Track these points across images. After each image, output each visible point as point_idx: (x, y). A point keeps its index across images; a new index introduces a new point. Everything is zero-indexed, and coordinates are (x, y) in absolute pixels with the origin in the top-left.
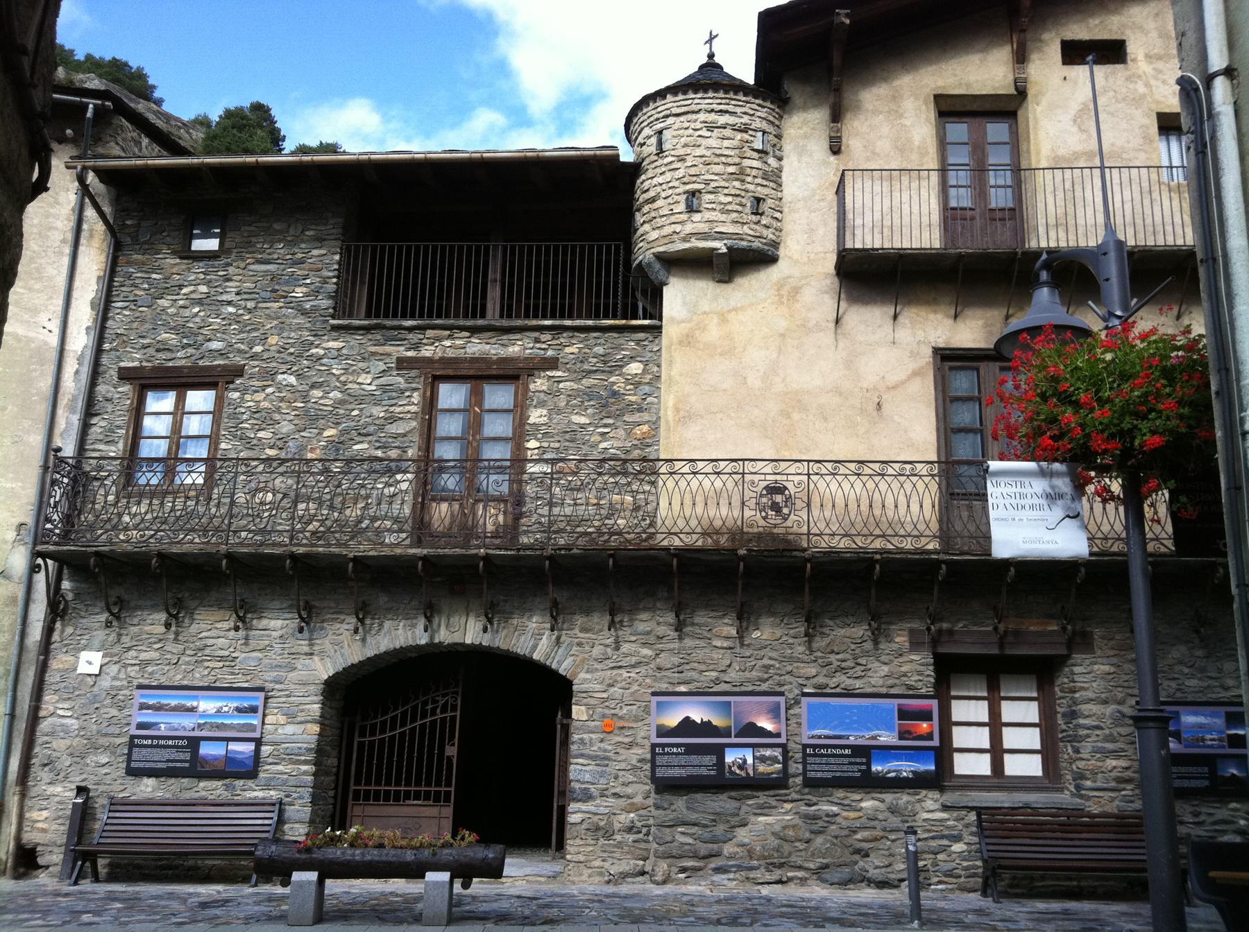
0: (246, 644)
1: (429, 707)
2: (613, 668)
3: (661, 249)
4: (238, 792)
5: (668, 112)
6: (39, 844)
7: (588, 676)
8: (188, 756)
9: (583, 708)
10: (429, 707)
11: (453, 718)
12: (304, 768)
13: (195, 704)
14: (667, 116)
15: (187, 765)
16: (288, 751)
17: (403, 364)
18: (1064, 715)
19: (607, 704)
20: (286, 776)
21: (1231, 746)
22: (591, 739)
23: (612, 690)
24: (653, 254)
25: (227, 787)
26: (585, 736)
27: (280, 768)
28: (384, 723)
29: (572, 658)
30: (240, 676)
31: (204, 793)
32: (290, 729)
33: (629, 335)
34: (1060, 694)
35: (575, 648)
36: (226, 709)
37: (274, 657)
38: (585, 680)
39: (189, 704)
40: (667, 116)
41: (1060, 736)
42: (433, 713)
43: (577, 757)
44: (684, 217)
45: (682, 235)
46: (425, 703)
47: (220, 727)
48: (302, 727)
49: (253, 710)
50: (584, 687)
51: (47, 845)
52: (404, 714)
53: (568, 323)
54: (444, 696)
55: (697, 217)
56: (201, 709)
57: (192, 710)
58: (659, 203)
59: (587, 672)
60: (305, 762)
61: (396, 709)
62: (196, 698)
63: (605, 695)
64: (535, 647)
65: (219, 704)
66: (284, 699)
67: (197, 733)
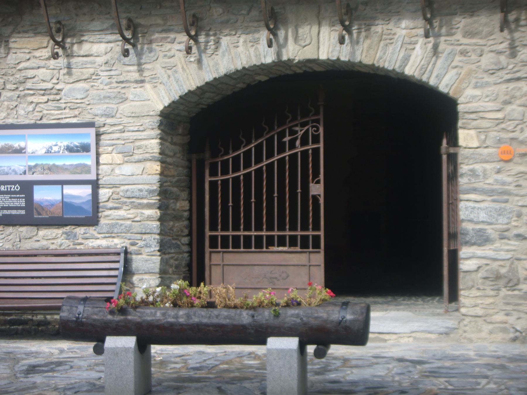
0: (69, 74)
1: (287, 139)
2: (509, 81)
4: (80, 241)
7: (477, 92)
8: (22, 203)
9: (472, 132)
10: (287, 139)
11: (316, 151)
12: (148, 212)
13: (22, 144)
15: (23, 212)
16: (129, 194)
19: (503, 126)
20: (129, 222)
22: (485, 170)
23: (509, 108)
25: (68, 235)
26: (477, 167)
27: (121, 213)
28: (236, 159)
29: (454, 71)
30: (67, 111)
31: (44, 243)
32: (128, 169)
35: (458, 58)
36: (55, 149)
37: (101, 87)
38: (474, 97)
39: (17, 144)
42: (292, 146)
43: (468, 192)
46: (282, 135)
47: (51, 169)
48: (141, 166)
49: (85, 148)
50: (473, 106)
52: (259, 148)
54: (303, 125)
56: (29, 150)
57: (20, 151)
59: (476, 87)
60: (149, 206)
61: (249, 142)
62: (23, 137)
63: (500, 115)
64: (406, 59)
65: (48, 143)
66: (117, 135)
67: (29, 177)
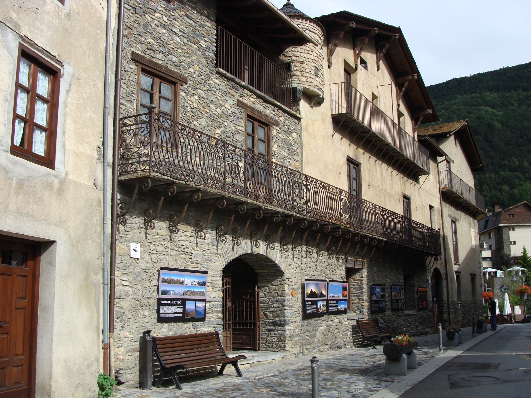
0: (197, 246)
3: (307, 87)
5: (308, 28)
6: (121, 369)
8: (181, 310)
13: (183, 279)
14: (307, 29)
15: (181, 315)
17: (240, 104)
18: (355, 288)
20: (213, 319)
21: (382, 298)
24: (303, 87)
25: (195, 327)
30: (195, 264)
31: (186, 331)
33: (293, 119)
34: (353, 281)
36: (194, 283)
37: (206, 254)
39: (181, 279)
40: (307, 29)
41: (353, 295)
44: (314, 77)
45: (313, 84)
47: (193, 293)
51: (125, 369)
53: (283, 106)
55: (317, 79)
56: (185, 283)
57: (182, 283)
58: (305, 66)
62: (183, 276)
65: (192, 280)
67: (185, 297)
